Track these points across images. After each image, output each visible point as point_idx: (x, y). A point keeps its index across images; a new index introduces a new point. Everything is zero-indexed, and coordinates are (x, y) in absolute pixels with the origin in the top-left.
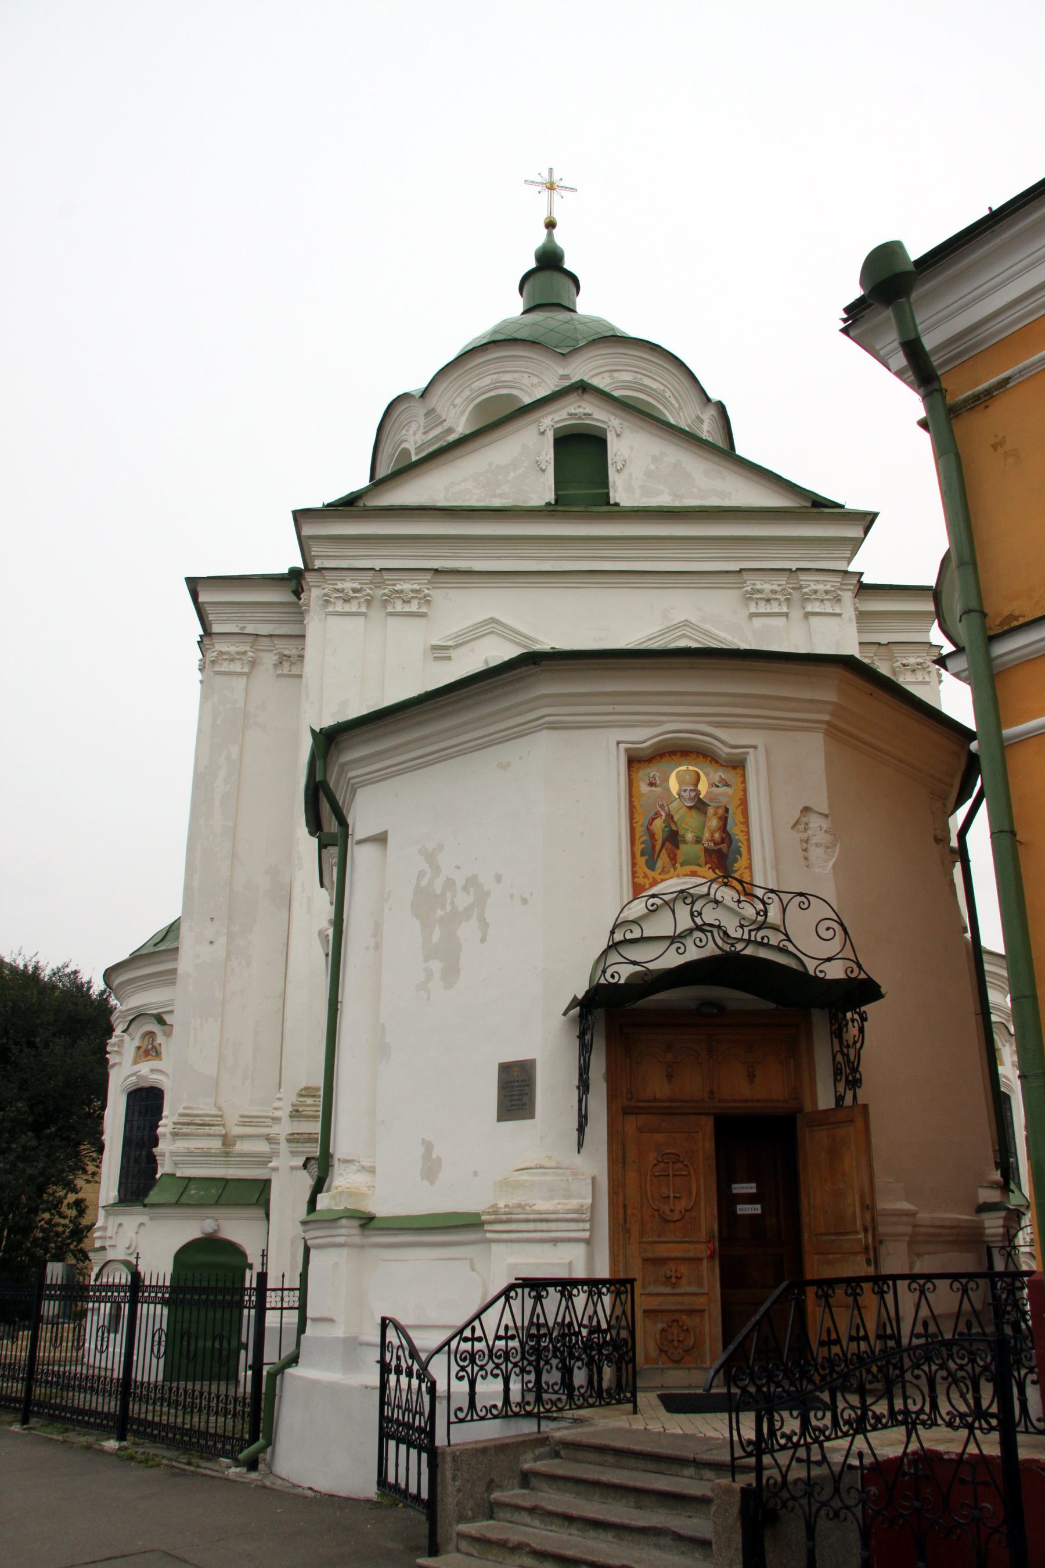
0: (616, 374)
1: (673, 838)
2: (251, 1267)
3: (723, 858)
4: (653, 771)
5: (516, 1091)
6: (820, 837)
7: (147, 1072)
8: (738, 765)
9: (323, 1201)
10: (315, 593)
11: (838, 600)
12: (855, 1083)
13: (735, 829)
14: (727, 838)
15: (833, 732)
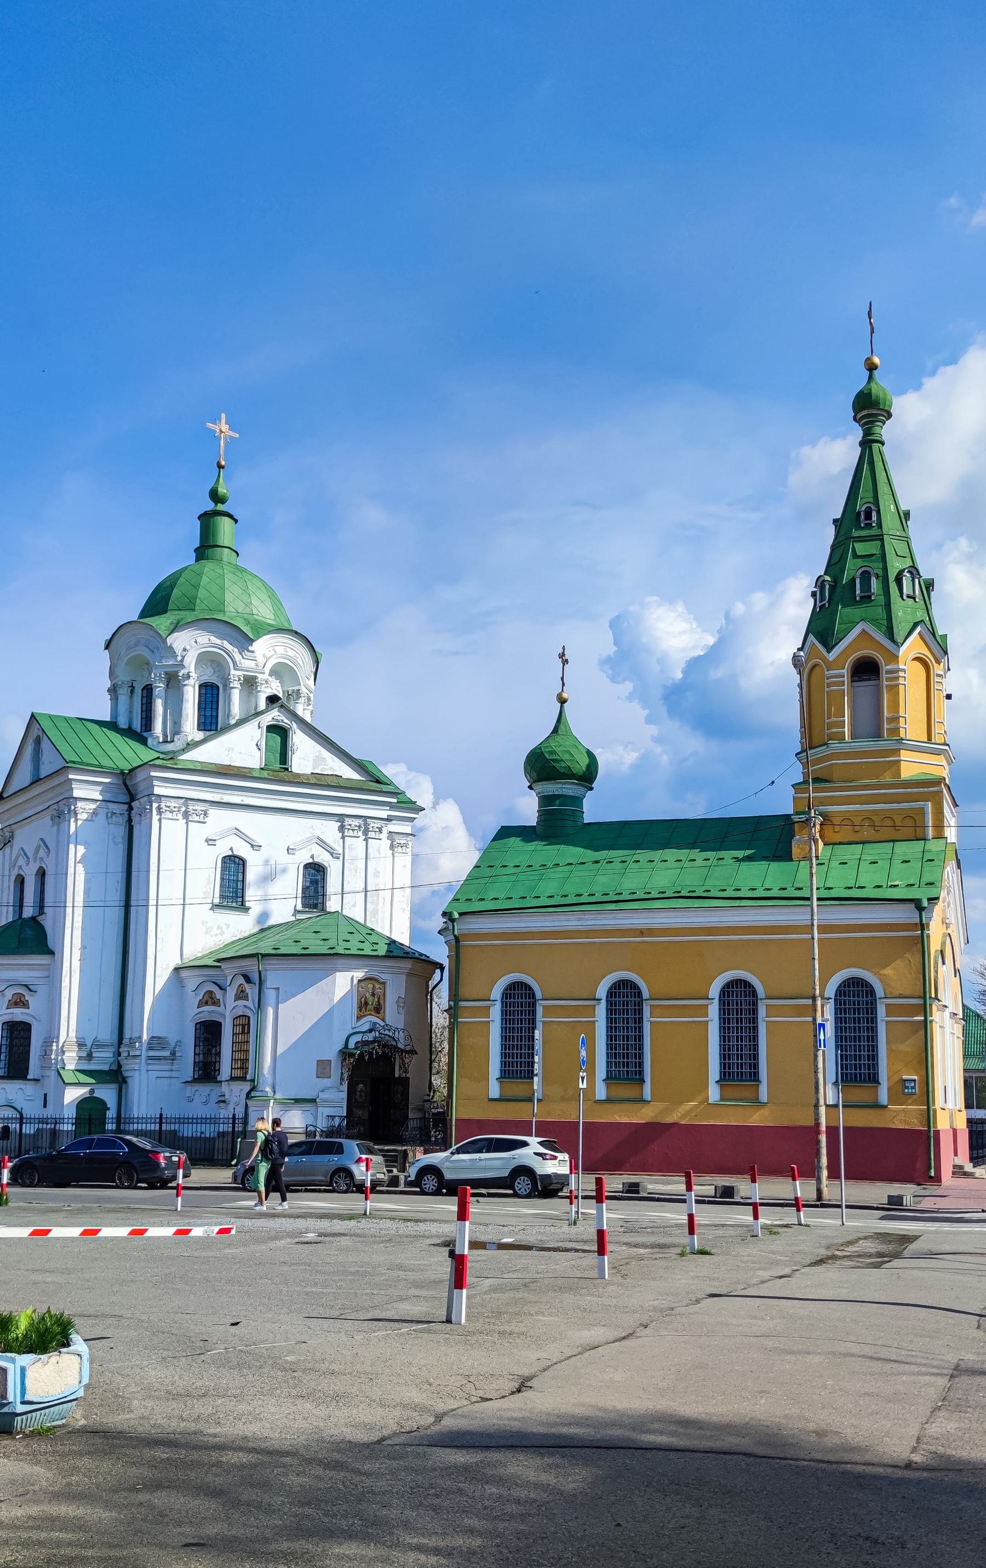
0: (276, 648)
1: (366, 1003)
2: (109, 1109)
3: (378, 1010)
4: (362, 984)
5: (323, 1068)
6: (402, 1005)
7: (19, 1014)
8: (384, 983)
9: (253, 1094)
10: (155, 805)
11: (381, 831)
12: (406, 1071)
13: (382, 1002)
14: (379, 1004)
15: (408, 975)
